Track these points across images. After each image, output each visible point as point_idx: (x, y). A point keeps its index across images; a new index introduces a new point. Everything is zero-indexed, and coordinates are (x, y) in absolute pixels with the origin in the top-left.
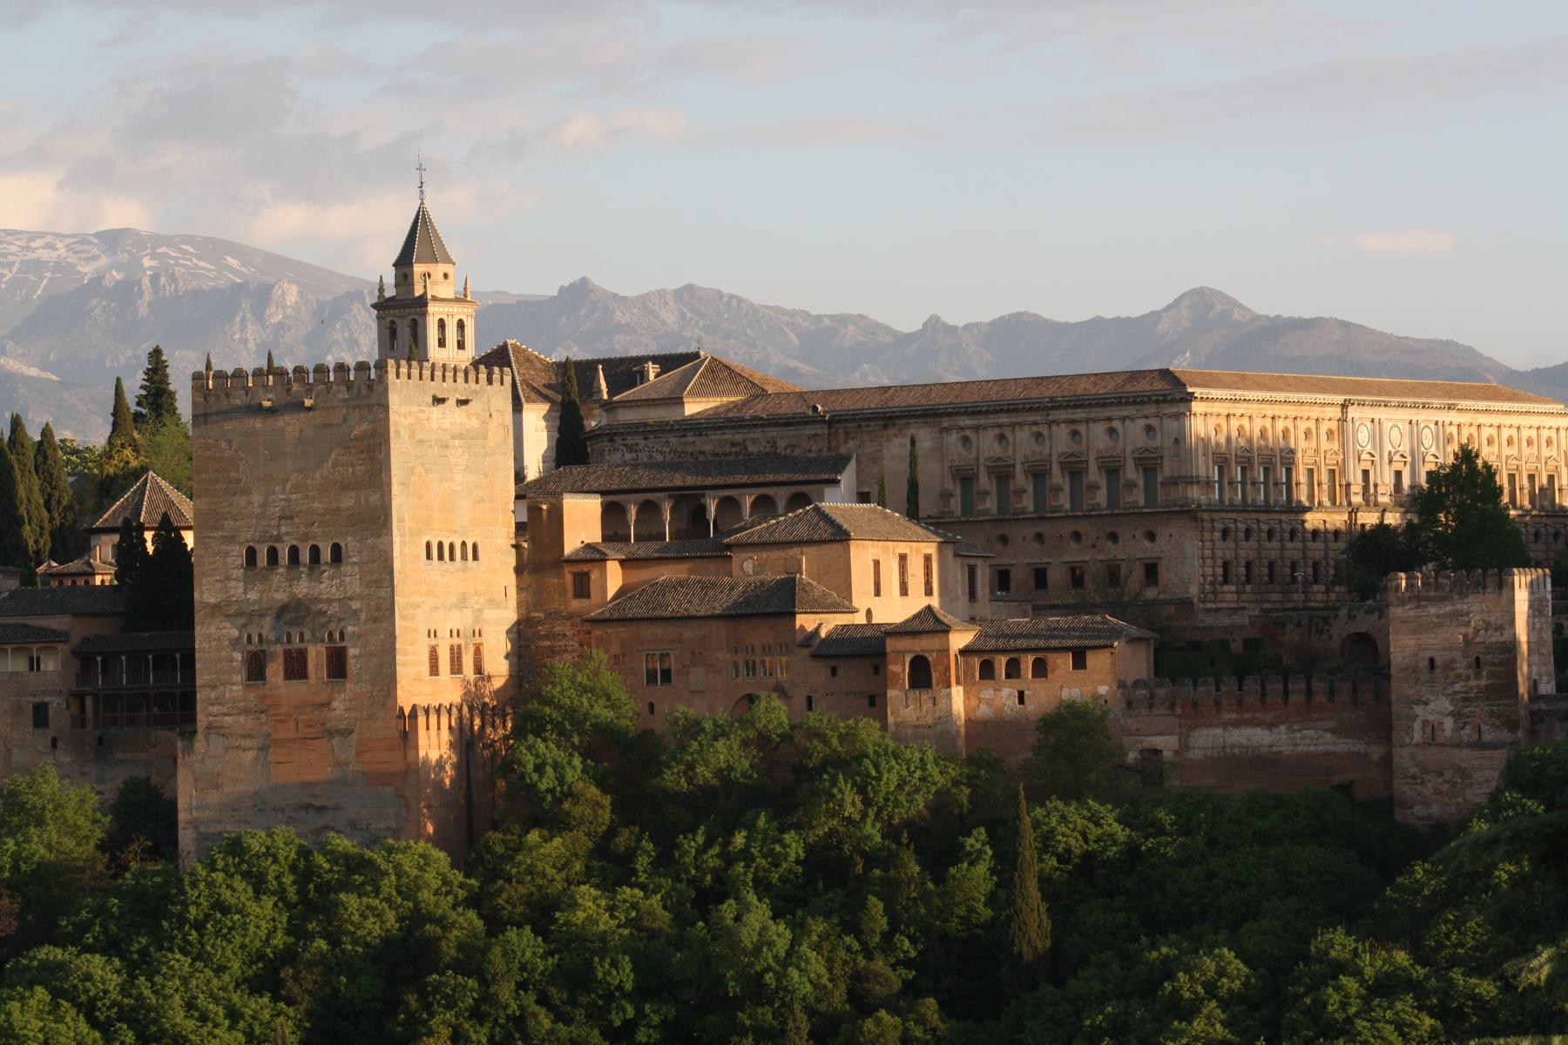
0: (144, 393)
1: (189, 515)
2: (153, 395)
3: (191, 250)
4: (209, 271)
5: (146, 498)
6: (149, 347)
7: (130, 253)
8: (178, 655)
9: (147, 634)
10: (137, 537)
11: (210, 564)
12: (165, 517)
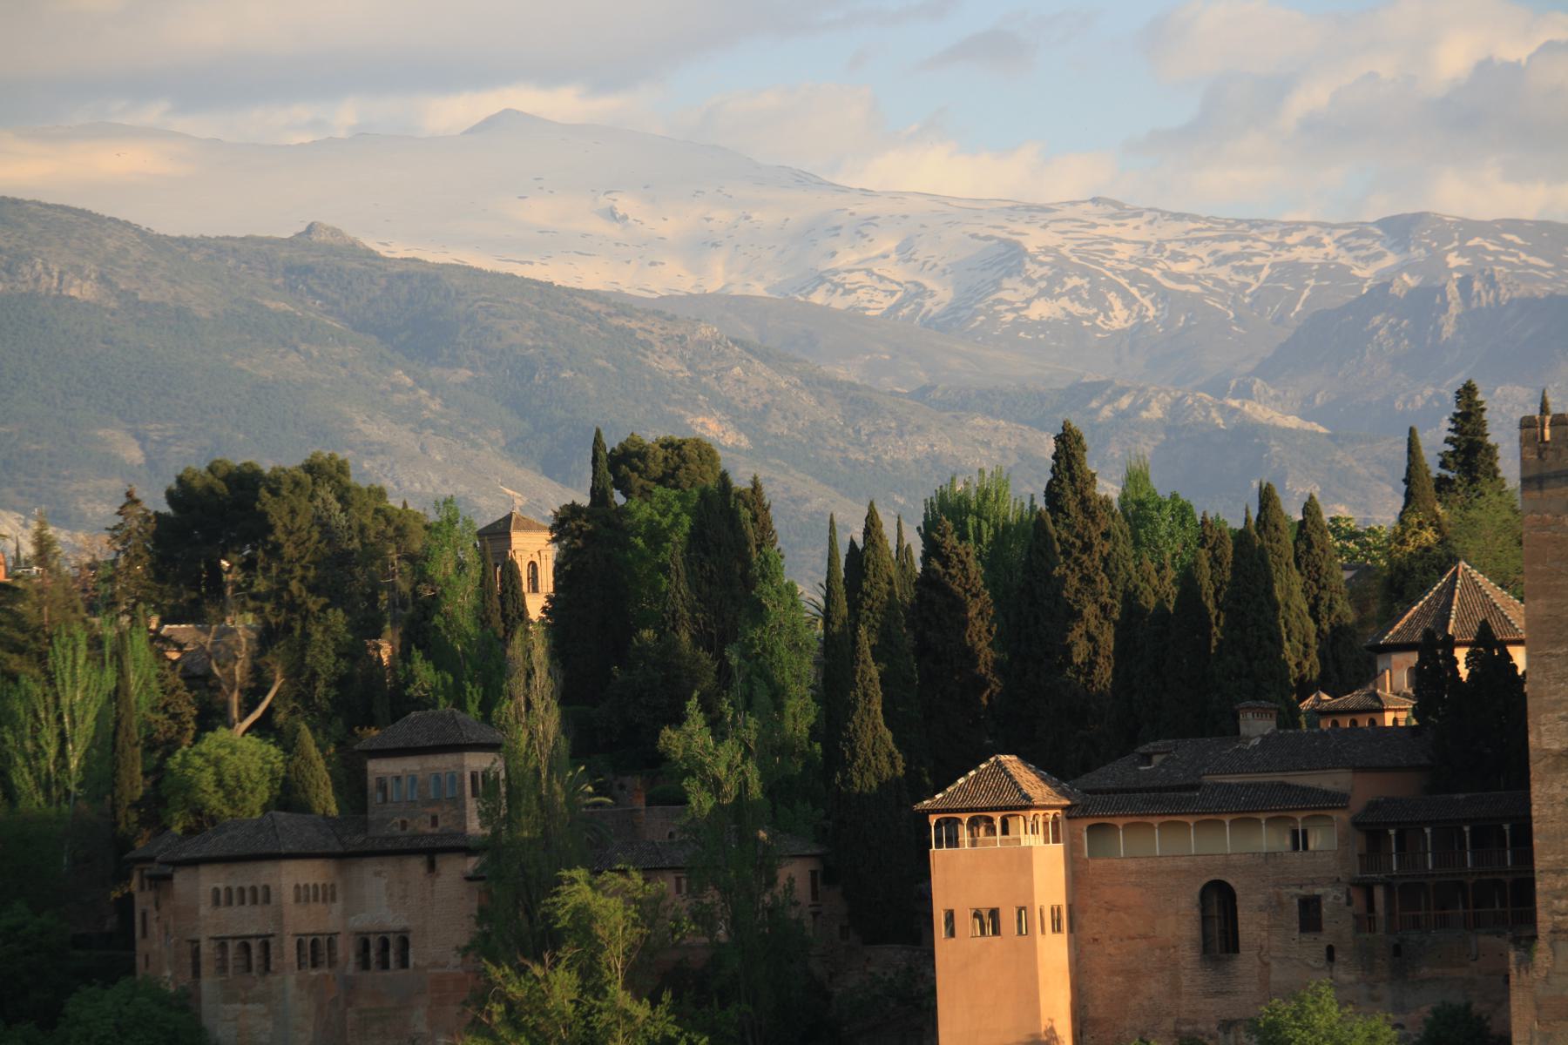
0: (1450, 448)
1: (1519, 623)
2: (1463, 452)
3: (1518, 240)
4: (1544, 269)
5: (1456, 600)
6: (1458, 381)
7: (1428, 248)
8: (1507, 827)
9: (1461, 796)
10: (1444, 656)
11: (1551, 694)
12: (1485, 627)
